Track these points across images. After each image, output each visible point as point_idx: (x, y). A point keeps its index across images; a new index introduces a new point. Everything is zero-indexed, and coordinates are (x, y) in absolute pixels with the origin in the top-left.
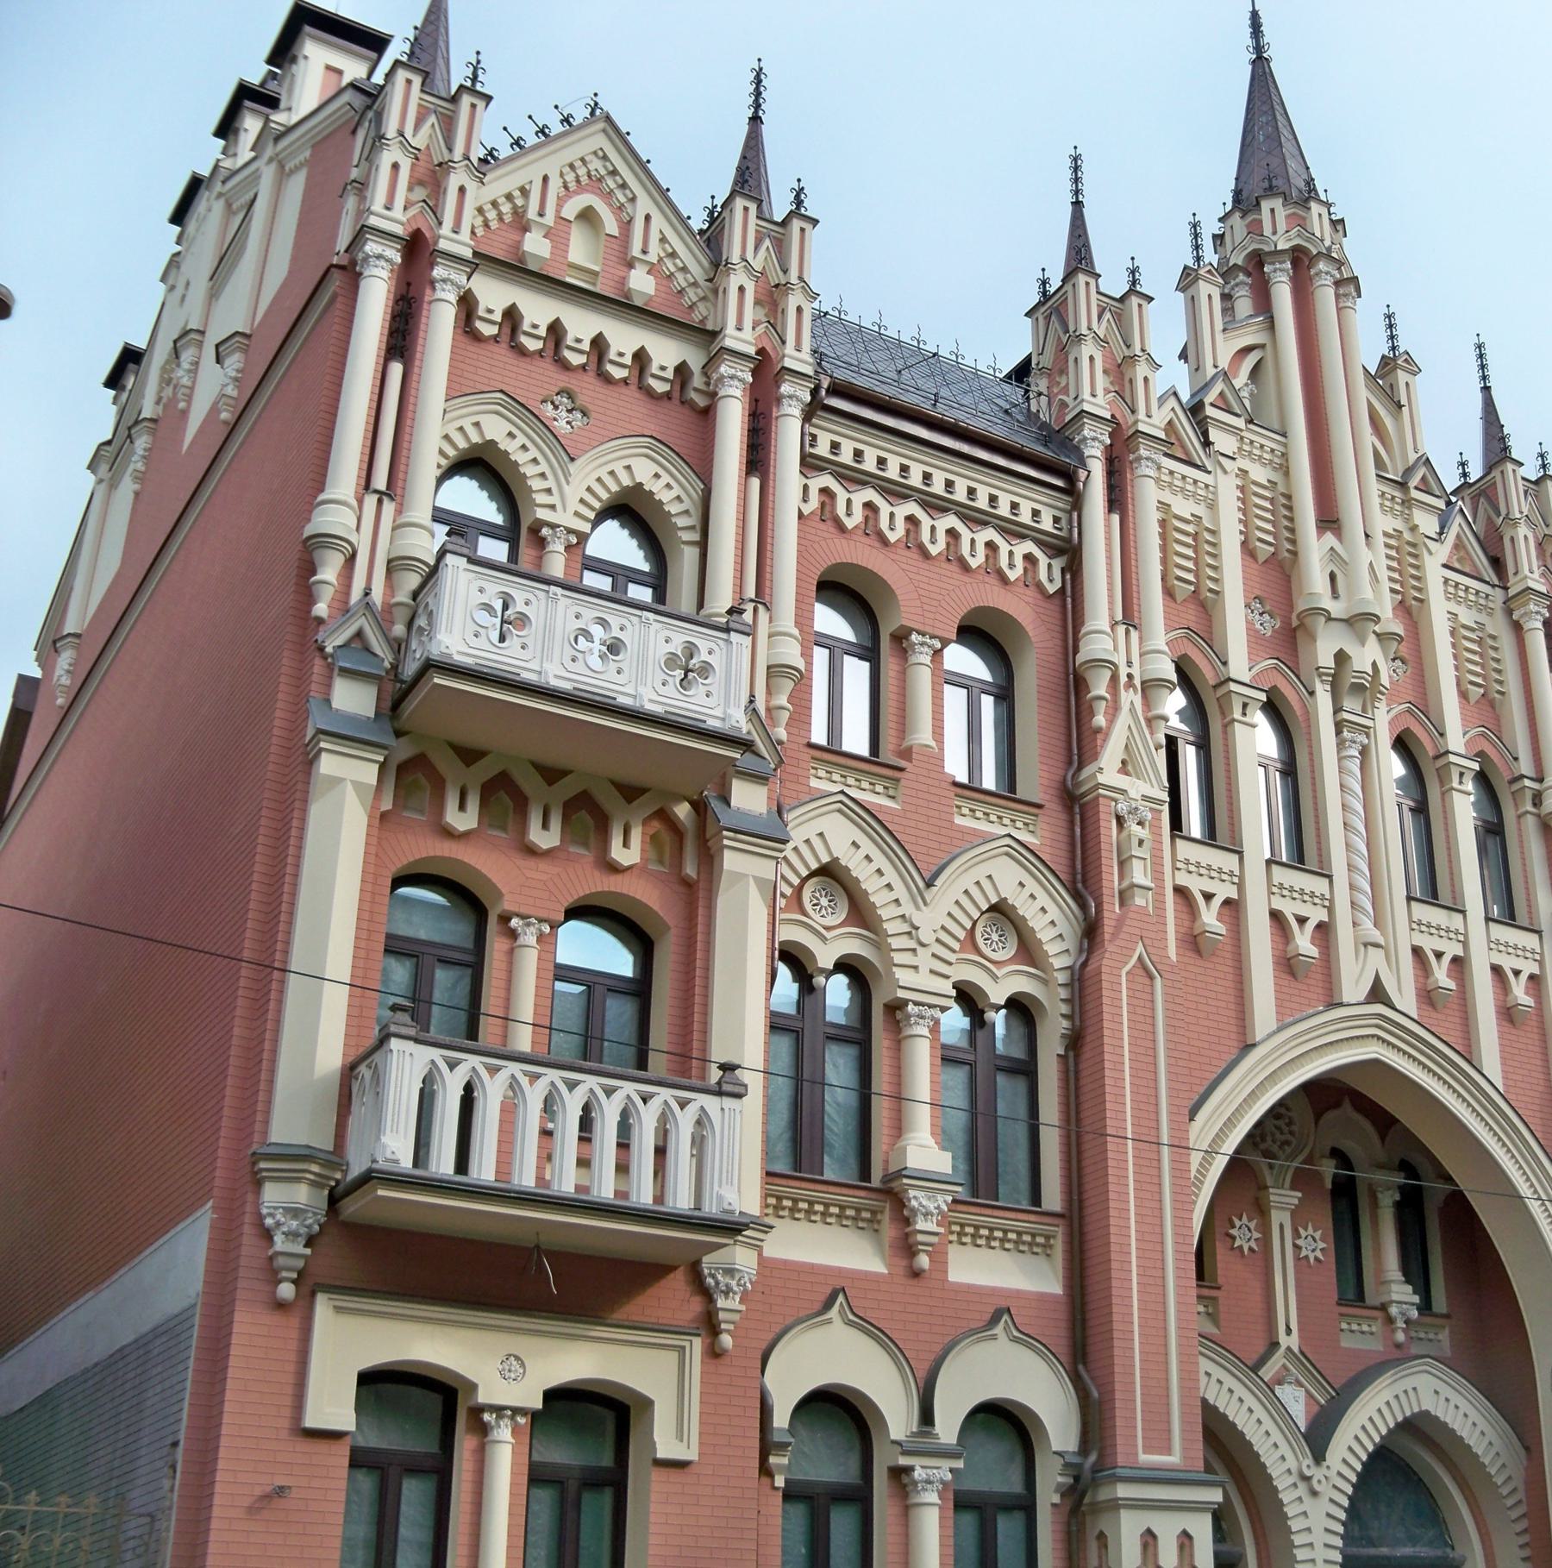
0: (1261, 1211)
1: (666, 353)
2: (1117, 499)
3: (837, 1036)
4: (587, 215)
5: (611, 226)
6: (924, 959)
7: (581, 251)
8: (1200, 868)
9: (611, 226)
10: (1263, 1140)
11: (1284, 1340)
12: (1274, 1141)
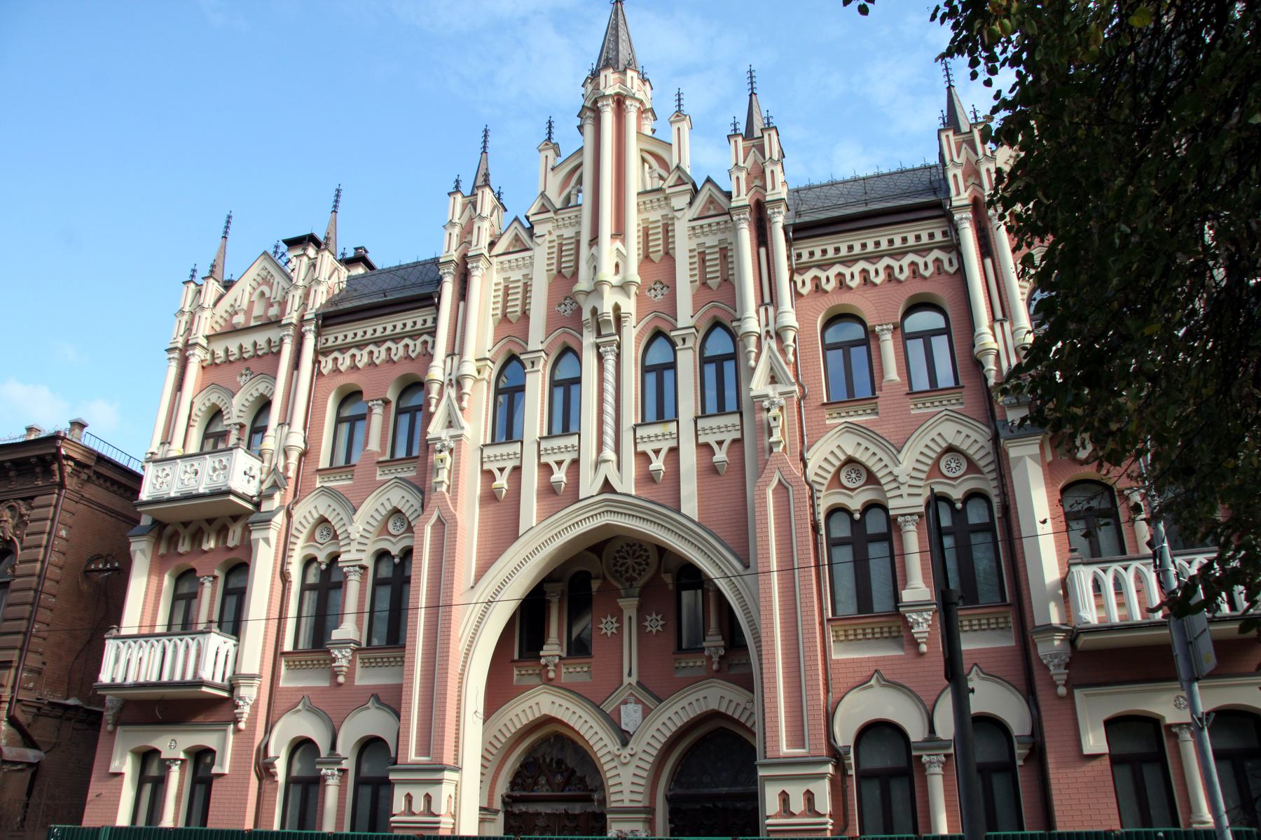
0: (618, 613)
1: (274, 334)
2: (463, 293)
5: (267, 295)
6: (354, 546)
7: (258, 310)
10: (627, 571)
11: (626, 680)
12: (634, 570)
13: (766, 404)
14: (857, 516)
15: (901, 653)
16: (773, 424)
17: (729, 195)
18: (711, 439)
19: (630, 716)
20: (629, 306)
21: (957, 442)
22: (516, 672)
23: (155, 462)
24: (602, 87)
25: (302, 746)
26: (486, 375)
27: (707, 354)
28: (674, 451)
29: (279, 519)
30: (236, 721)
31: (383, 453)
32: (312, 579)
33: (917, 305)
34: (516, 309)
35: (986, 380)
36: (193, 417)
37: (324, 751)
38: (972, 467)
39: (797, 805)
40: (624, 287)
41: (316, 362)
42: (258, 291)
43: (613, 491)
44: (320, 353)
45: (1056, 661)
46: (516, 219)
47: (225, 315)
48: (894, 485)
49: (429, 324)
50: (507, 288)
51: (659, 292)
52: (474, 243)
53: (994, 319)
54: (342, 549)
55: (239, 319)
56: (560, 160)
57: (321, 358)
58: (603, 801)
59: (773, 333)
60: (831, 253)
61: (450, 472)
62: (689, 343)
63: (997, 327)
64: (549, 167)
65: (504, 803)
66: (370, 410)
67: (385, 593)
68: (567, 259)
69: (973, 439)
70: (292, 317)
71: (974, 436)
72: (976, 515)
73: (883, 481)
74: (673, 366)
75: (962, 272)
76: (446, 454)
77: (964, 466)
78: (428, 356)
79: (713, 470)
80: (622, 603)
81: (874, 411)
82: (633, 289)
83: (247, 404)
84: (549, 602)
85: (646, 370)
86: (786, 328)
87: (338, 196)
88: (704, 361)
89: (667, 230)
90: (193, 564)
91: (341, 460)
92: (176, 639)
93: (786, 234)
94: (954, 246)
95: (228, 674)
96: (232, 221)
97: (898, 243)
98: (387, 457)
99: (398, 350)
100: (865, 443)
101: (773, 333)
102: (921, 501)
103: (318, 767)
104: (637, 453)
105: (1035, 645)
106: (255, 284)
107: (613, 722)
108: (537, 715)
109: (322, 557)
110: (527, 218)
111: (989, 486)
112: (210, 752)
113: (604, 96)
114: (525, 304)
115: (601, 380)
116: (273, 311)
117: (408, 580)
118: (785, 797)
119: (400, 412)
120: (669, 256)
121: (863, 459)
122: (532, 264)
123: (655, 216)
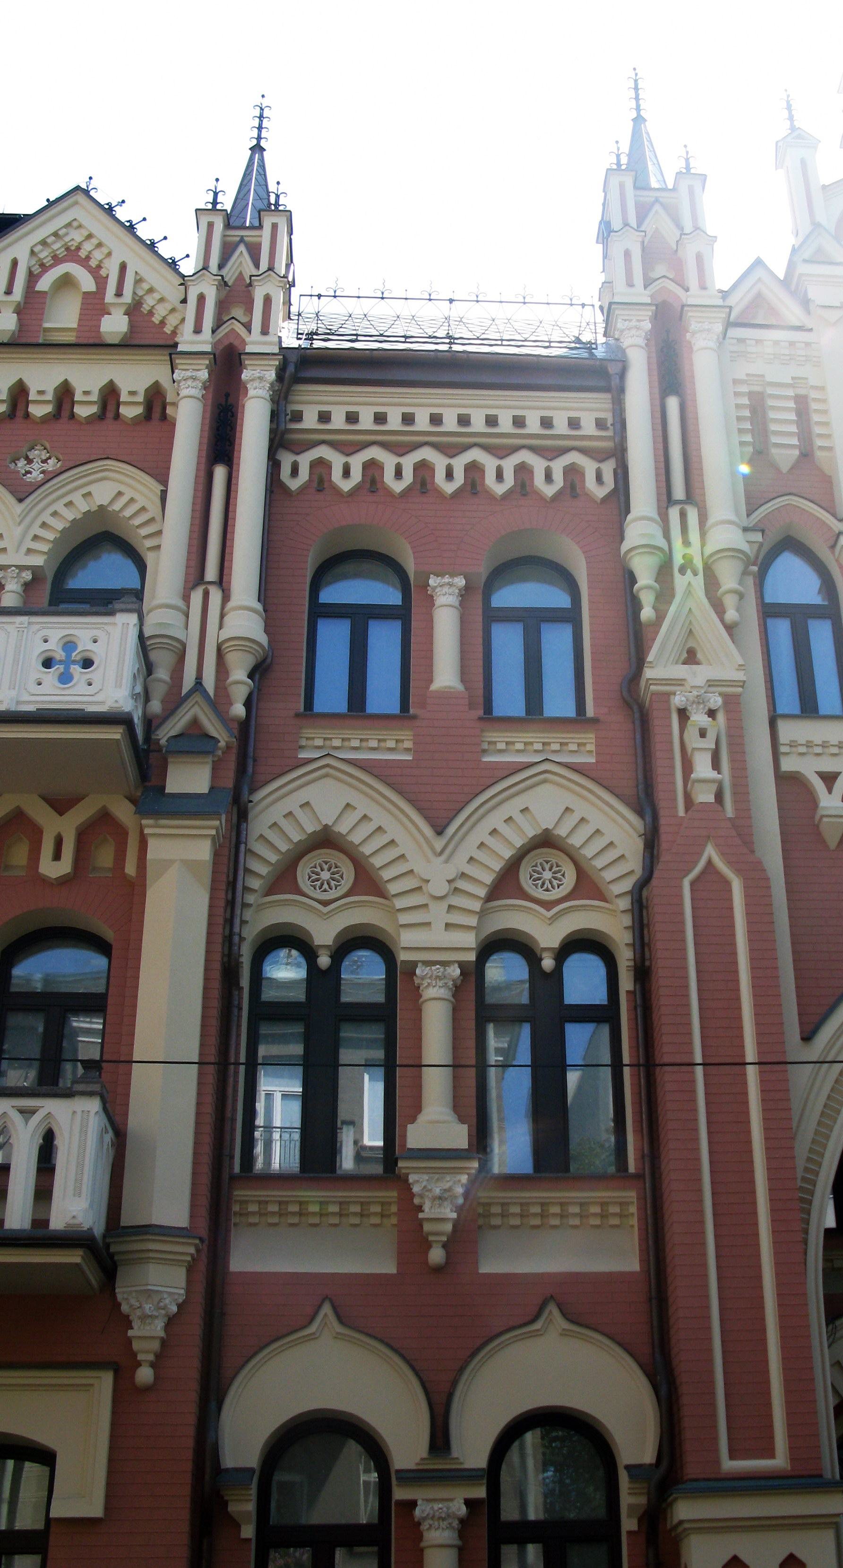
1: (134, 377)
3: (363, 1014)
4: (66, 281)
9: (88, 284)
44: (280, 440)
46: (758, 263)
49: (588, 428)
52: (692, 281)
54: (404, 919)
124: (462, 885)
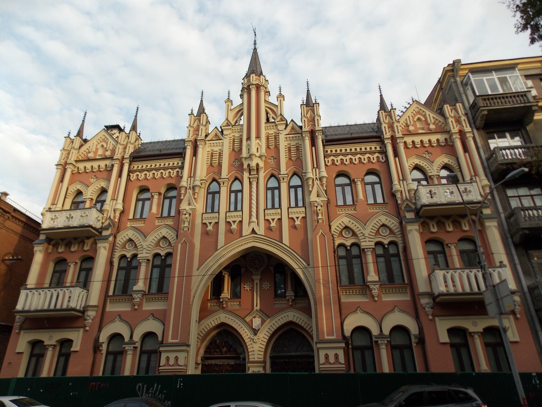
1: (108, 162)
2: (195, 153)
5: (105, 146)
6: (145, 251)
7: (100, 152)
8: (210, 218)
11: (255, 308)
13: (316, 204)
14: (349, 248)
15: (367, 300)
16: (319, 212)
17: (301, 127)
18: (294, 216)
19: (257, 322)
20: (261, 164)
21: (386, 223)
22: (209, 305)
23: (51, 211)
24: (251, 80)
25: (116, 337)
26: (203, 186)
27: (291, 184)
28: (280, 220)
29: (111, 239)
30: (85, 326)
31: (158, 214)
32: (124, 264)
33: (370, 172)
34: (216, 161)
35: (397, 201)
36: (68, 194)
37: (127, 339)
38: (391, 232)
39: (332, 359)
40: (260, 157)
41: (129, 175)
42: (101, 144)
43: (256, 234)
44: (130, 172)
45: (428, 306)
46: (216, 127)
47: (85, 153)
48: (364, 237)
49: (180, 164)
50: (212, 153)
51: (272, 160)
53: (399, 180)
54: (139, 252)
55: (91, 155)
56: (233, 107)
57: (131, 174)
58: (244, 359)
59: (318, 179)
60: (339, 151)
61: (189, 223)
62: (285, 180)
63: (401, 182)
64: (229, 109)
65: (202, 360)
66: (153, 196)
67: (156, 271)
68: (237, 145)
69: (393, 223)
70: (118, 156)
71: (392, 221)
72: (392, 250)
73: (359, 235)
74: (279, 188)
75: (387, 161)
76: (187, 216)
77: (388, 232)
78: (180, 177)
79: (295, 227)
80: (254, 277)
81: (355, 210)
82: (264, 158)
83: (95, 190)
84: (224, 276)
85: (267, 189)
86: (323, 177)
87: (137, 110)
88: (290, 187)
89: (276, 137)
90: (65, 256)
91: (138, 216)
92: (52, 290)
93: (323, 143)
94: (384, 152)
95: (83, 305)
96: (87, 114)
97: (363, 150)
98: (160, 216)
99: (166, 174)
100: (352, 221)
101: (318, 179)
102: (373, 244)
103: (124, 346)
104: (265, 220)
105: (419, 299)
106: (99, 141)
107: (250, 325)
108: (219, 322)
109: (129, 255)
110: (221, 127)
111: (399, 241)
112: (70, 342)
113: (252, 84)
114: (219, 160)
115: (251, 191)
116: (108, 154)
117: (170, 266)
118: (327, 356)
119: (165, 198)
120: (277, 147)
121: (352, 226)
122: (223, 145)
123: (272, 132)
124: (149, 246)
